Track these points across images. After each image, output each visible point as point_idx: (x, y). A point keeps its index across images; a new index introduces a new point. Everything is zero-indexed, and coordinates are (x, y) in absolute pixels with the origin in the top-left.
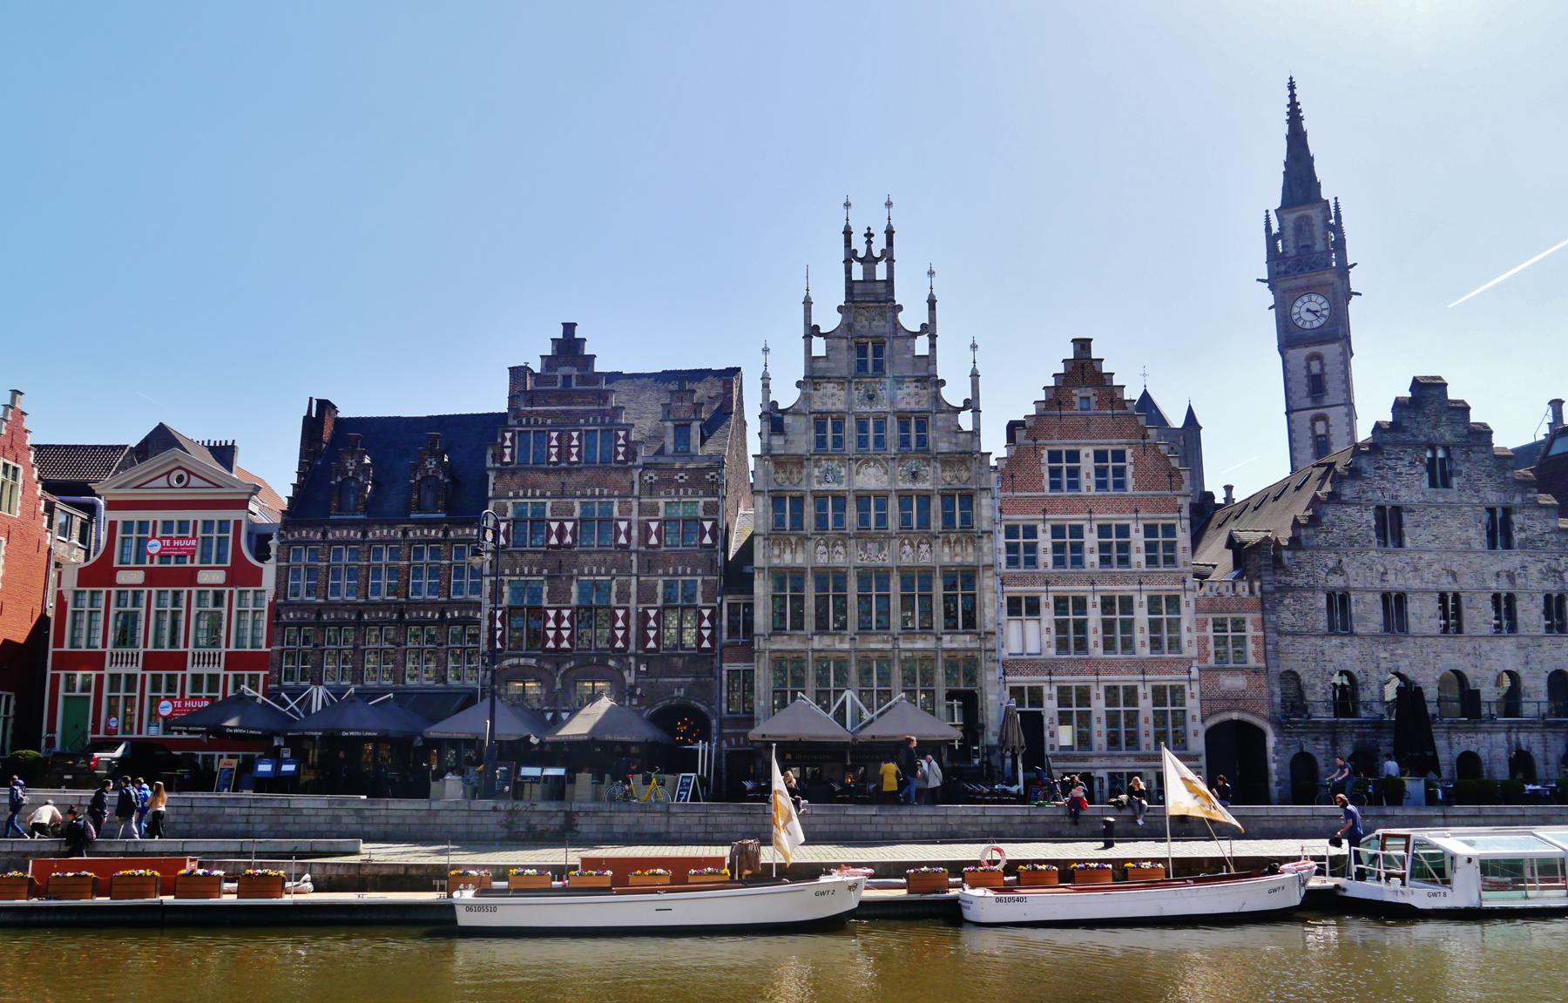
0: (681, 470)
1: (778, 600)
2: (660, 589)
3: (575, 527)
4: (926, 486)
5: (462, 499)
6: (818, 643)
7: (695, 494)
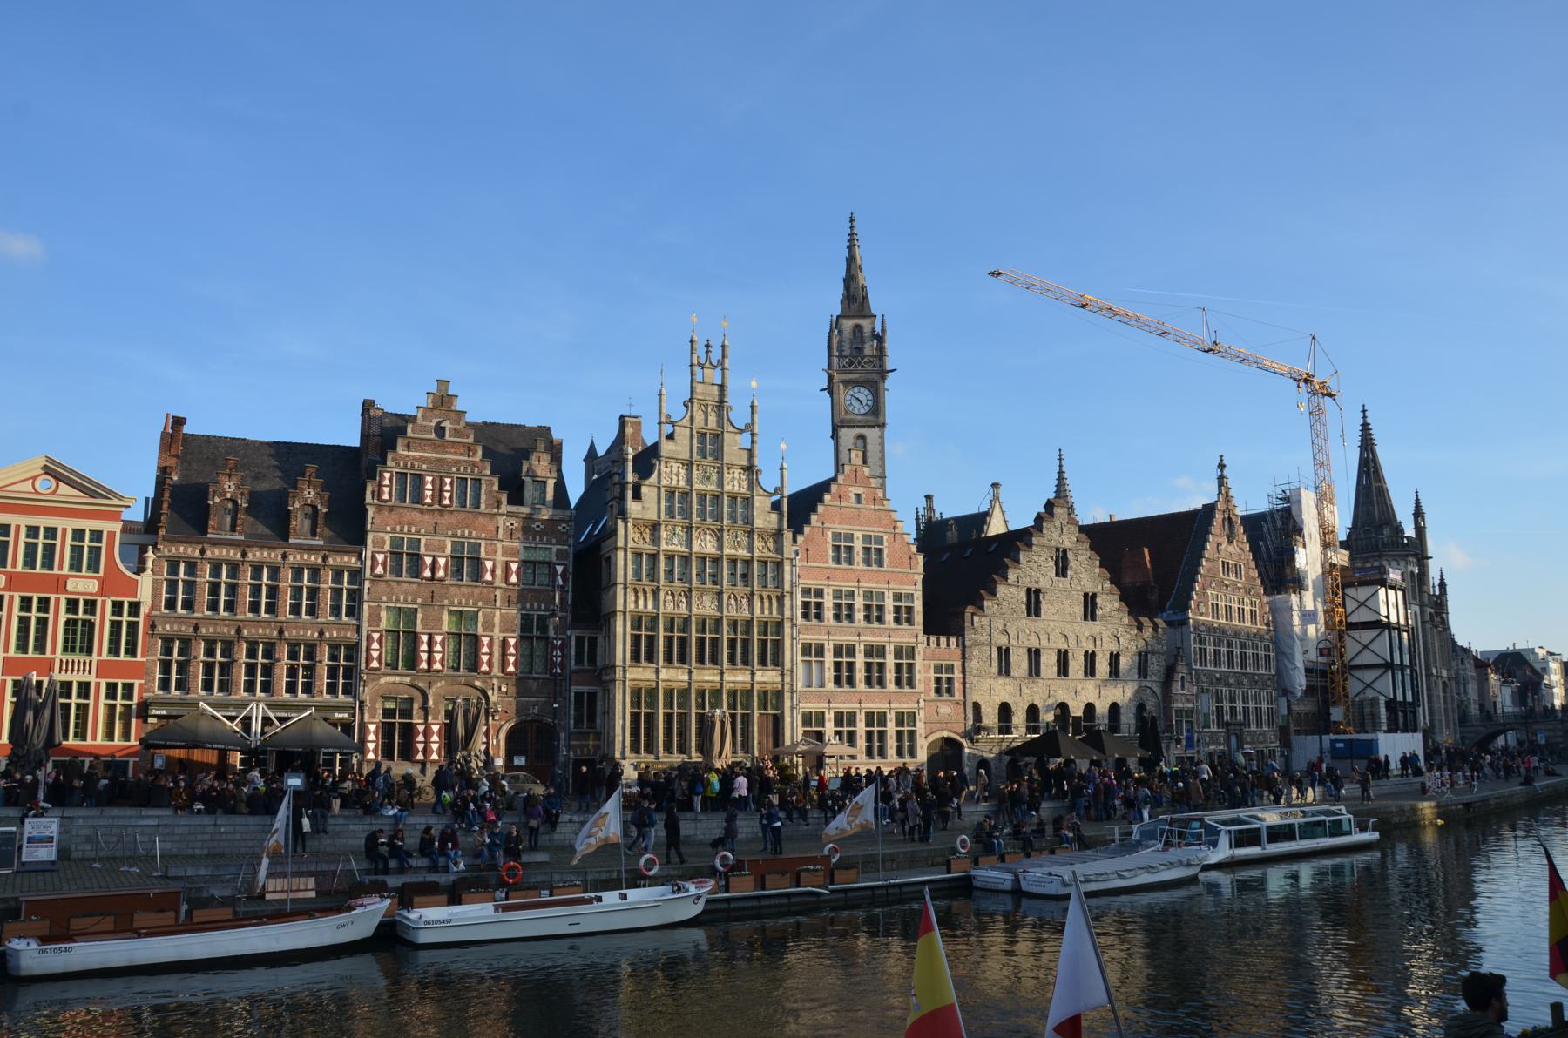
1: (636, 640)
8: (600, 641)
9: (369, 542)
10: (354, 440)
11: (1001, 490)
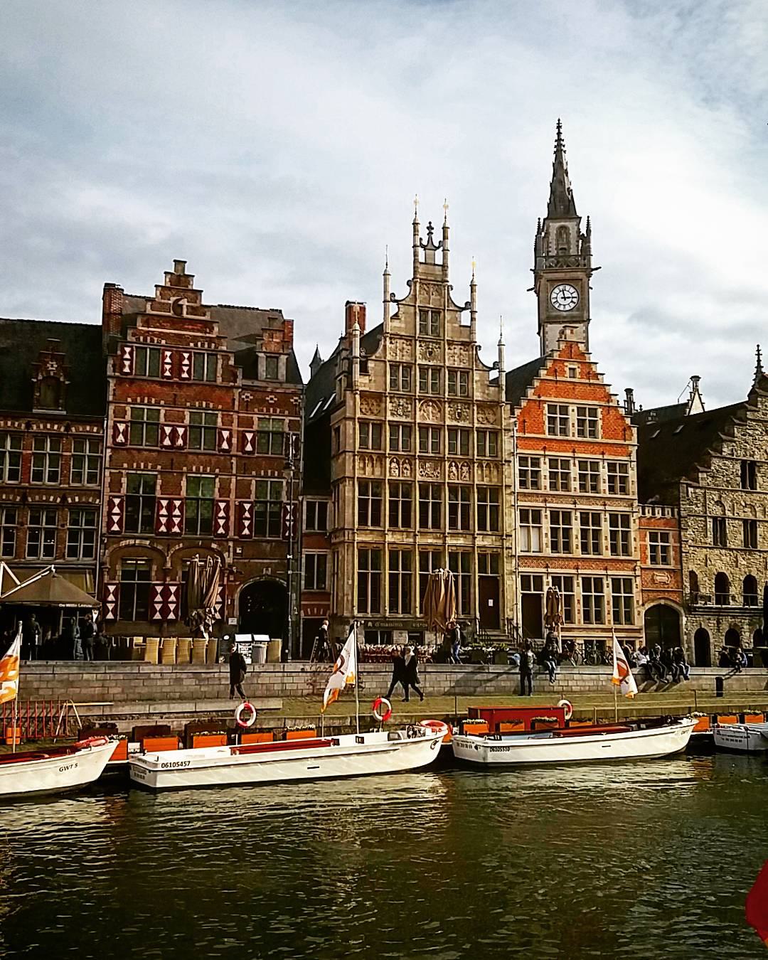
0: (272, 393)
1: (363, 503)
2: (253, 488)
3: (185, 432)
4: (467, 424)
5: (88, 401)
6: (389, 538)
7: (282, 413)
8: (330, 506)
9: (111, 412)
10: (98, 321)
11: (700, 383)
